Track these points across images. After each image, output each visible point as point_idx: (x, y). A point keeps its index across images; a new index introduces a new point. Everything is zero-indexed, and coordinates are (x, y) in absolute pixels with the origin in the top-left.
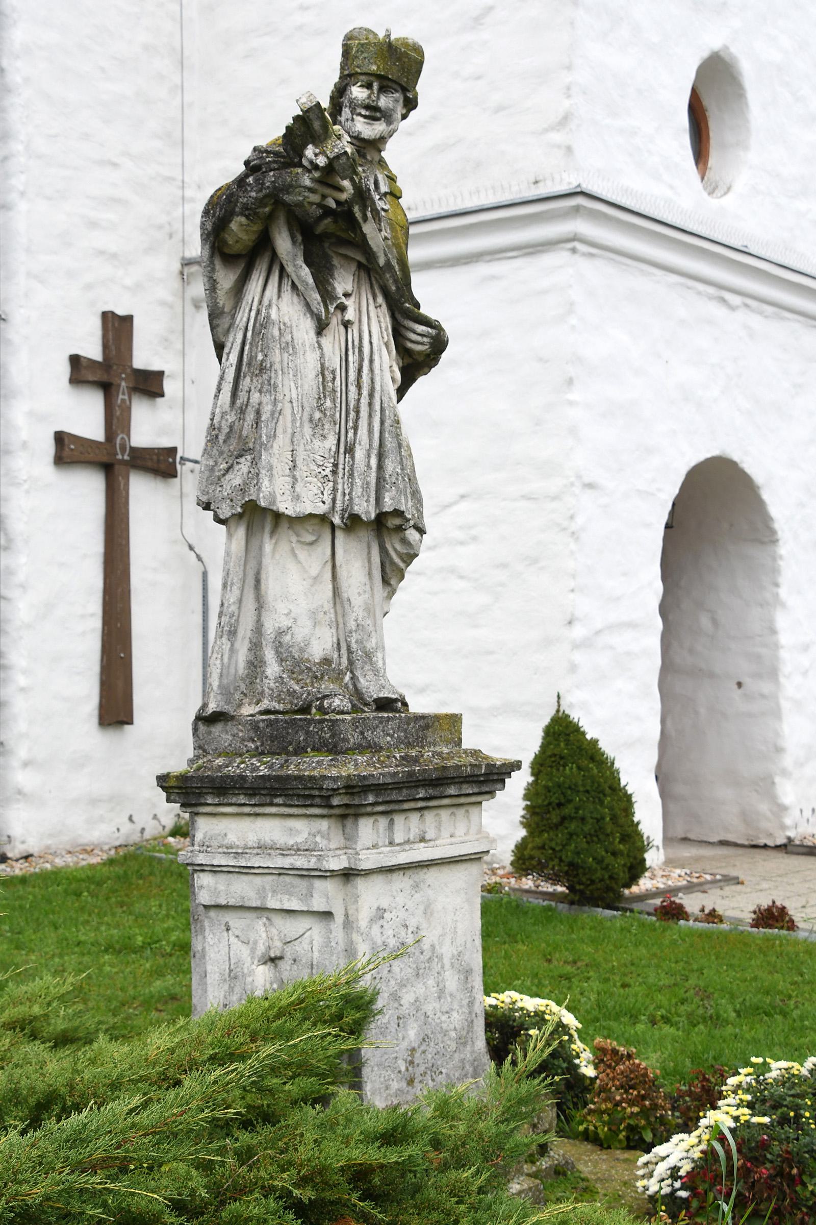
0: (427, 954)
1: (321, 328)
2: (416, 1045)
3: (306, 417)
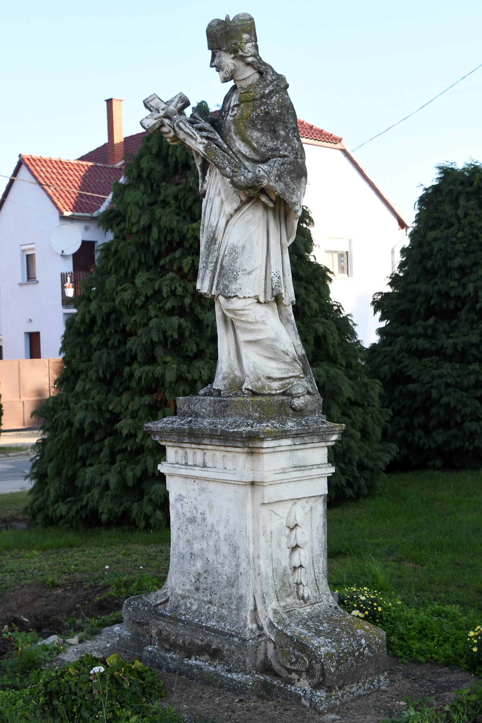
0: (209, 528)
2: (201, 572)
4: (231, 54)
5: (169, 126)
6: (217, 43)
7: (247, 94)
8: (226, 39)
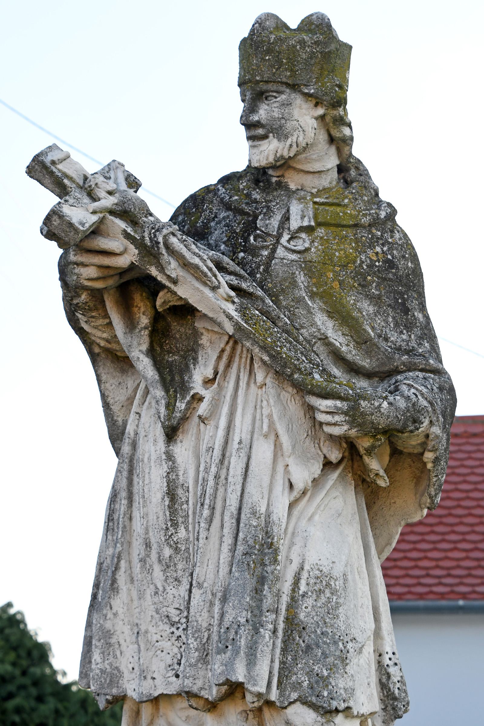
1: (171, 433)
3: (154, 555)
4: (316, 105)
5: (127, 236)
6: (292, 70)
7: (338, 209)
8: (322, 68)
